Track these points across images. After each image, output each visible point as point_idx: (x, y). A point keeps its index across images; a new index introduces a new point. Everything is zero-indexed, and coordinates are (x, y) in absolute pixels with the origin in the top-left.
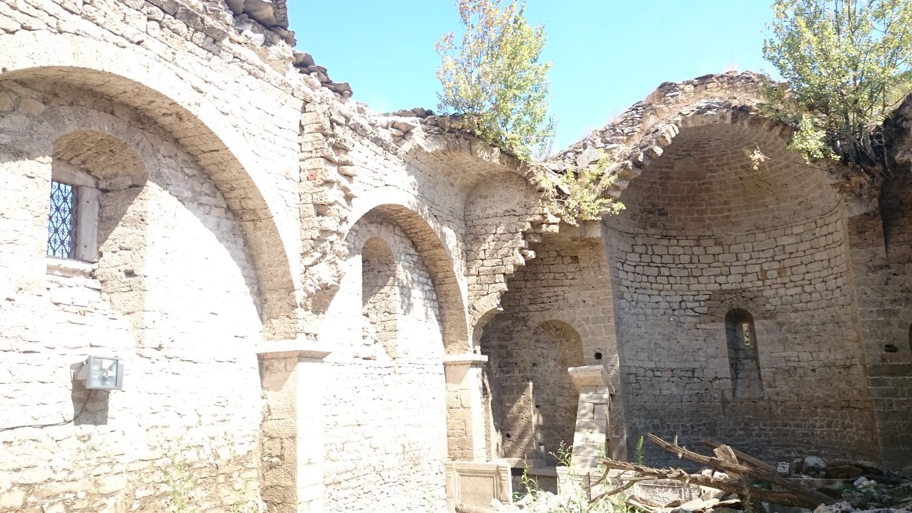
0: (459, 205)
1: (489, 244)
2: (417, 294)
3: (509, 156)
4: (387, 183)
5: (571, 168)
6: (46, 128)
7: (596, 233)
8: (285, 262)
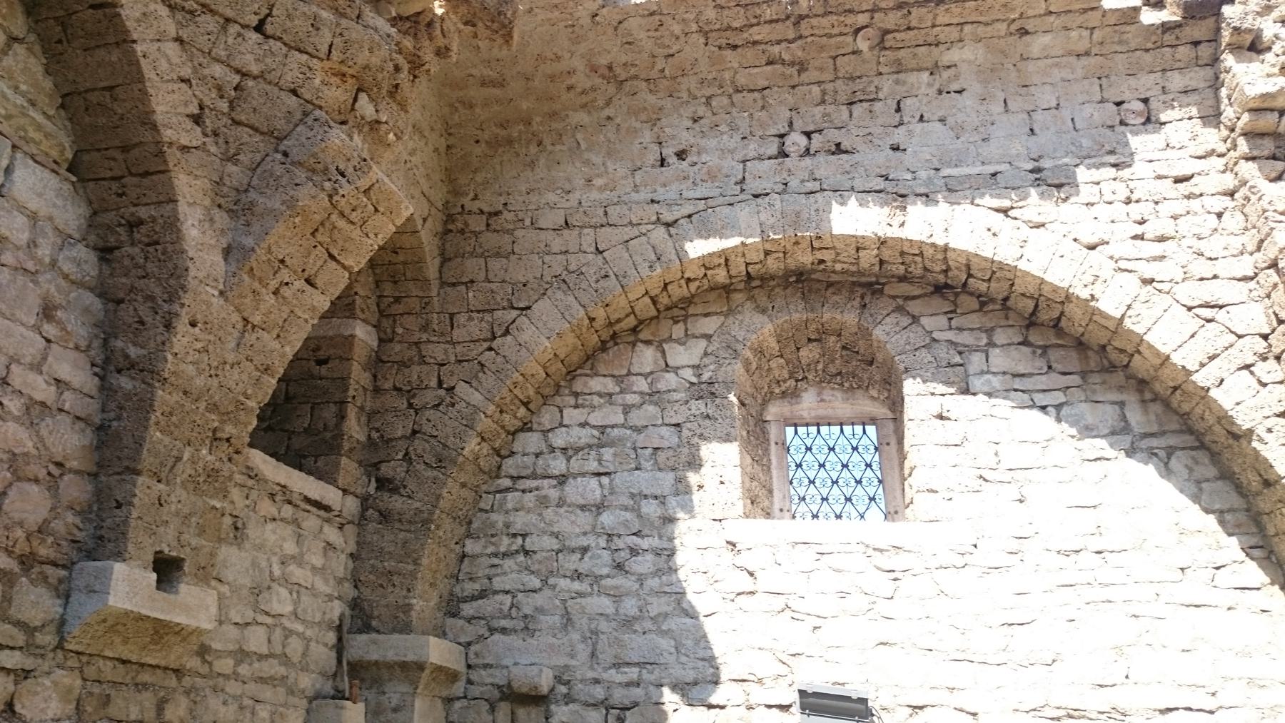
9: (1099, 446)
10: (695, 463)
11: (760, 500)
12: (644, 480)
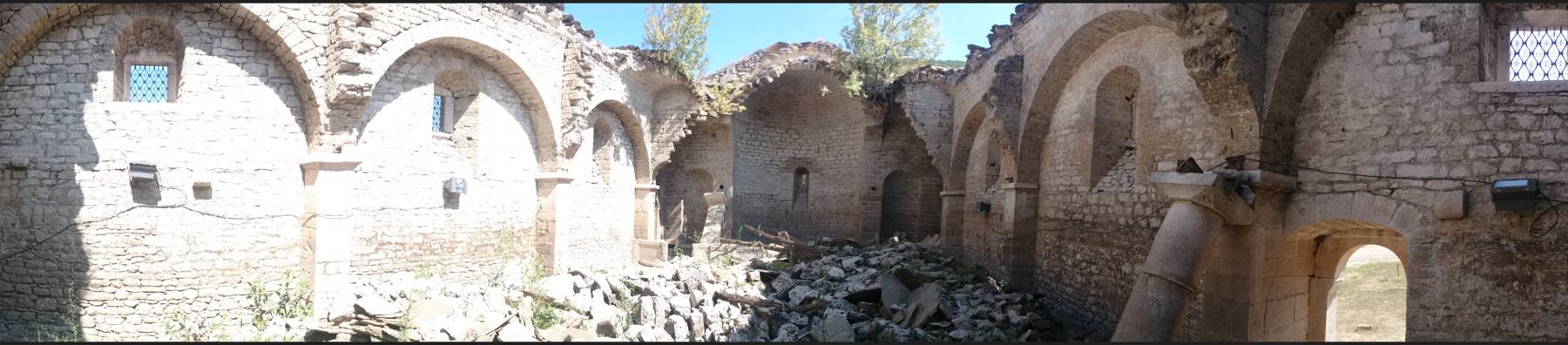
0: (650, 102)
1: (666, 125)
2: (623, 152)
3: (683, 76)
4: (611, 87)
5: (715, 82)
6: (432, 69)
7: (728, 122)
8: (552, 131)
9: (256, 80)
10: (94, 80)
11: (120, 94)
12: (70, 87)
